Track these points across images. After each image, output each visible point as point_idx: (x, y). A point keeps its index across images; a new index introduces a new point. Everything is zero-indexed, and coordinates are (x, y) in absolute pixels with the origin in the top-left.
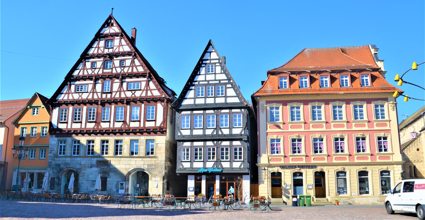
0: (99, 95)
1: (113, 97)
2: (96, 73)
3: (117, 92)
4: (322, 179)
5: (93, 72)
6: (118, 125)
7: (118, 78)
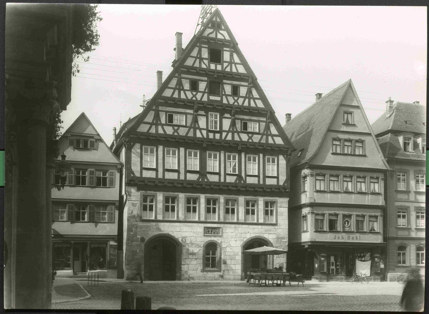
0: (204, 132)
1: (223, 139)
2: (199, 99)
3: (228, 132)
4: (326, 246)
5: (194, 96)
6: (231, 179)
7: (229, 112)
